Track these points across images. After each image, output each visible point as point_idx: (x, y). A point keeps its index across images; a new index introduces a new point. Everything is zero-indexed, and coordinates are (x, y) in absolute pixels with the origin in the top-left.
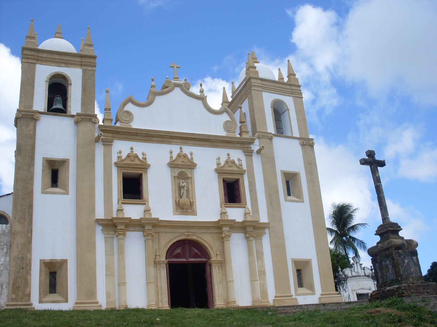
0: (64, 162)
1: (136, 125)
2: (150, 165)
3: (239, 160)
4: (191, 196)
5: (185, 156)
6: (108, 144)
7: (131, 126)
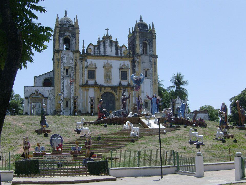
3: (128, 64)
5: (109, 64)
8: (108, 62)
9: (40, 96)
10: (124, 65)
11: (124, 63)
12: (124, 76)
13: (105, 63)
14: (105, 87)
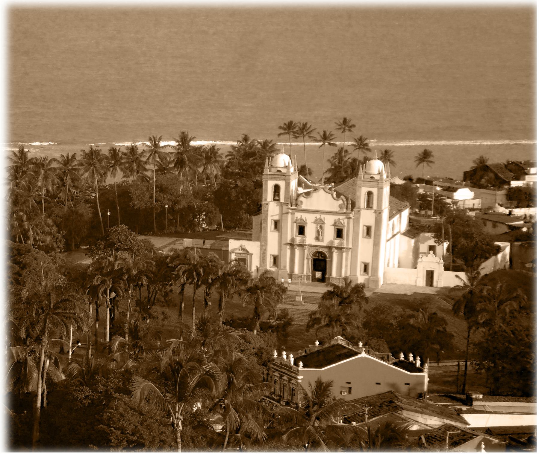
1: (304, 207)
6: (293, 214)
7: (301, 207)
12: (339, 234)
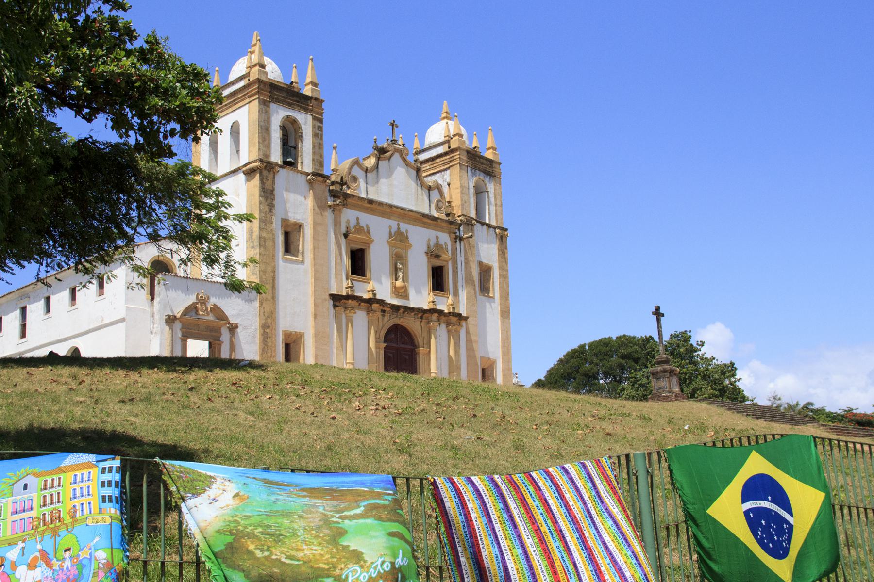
0: (299, 227)
2: (373, 240)
4: (405, 279)
5: (402, 234)
8: (399, 229)
9: (211, 317)
10: (437, 245)
11: (437, 237)
12: (438, 279)
13: (393, 231)
14: (395, 308)
